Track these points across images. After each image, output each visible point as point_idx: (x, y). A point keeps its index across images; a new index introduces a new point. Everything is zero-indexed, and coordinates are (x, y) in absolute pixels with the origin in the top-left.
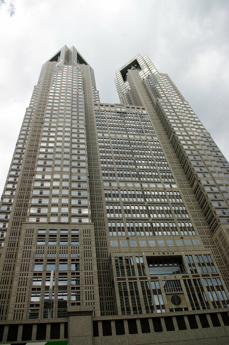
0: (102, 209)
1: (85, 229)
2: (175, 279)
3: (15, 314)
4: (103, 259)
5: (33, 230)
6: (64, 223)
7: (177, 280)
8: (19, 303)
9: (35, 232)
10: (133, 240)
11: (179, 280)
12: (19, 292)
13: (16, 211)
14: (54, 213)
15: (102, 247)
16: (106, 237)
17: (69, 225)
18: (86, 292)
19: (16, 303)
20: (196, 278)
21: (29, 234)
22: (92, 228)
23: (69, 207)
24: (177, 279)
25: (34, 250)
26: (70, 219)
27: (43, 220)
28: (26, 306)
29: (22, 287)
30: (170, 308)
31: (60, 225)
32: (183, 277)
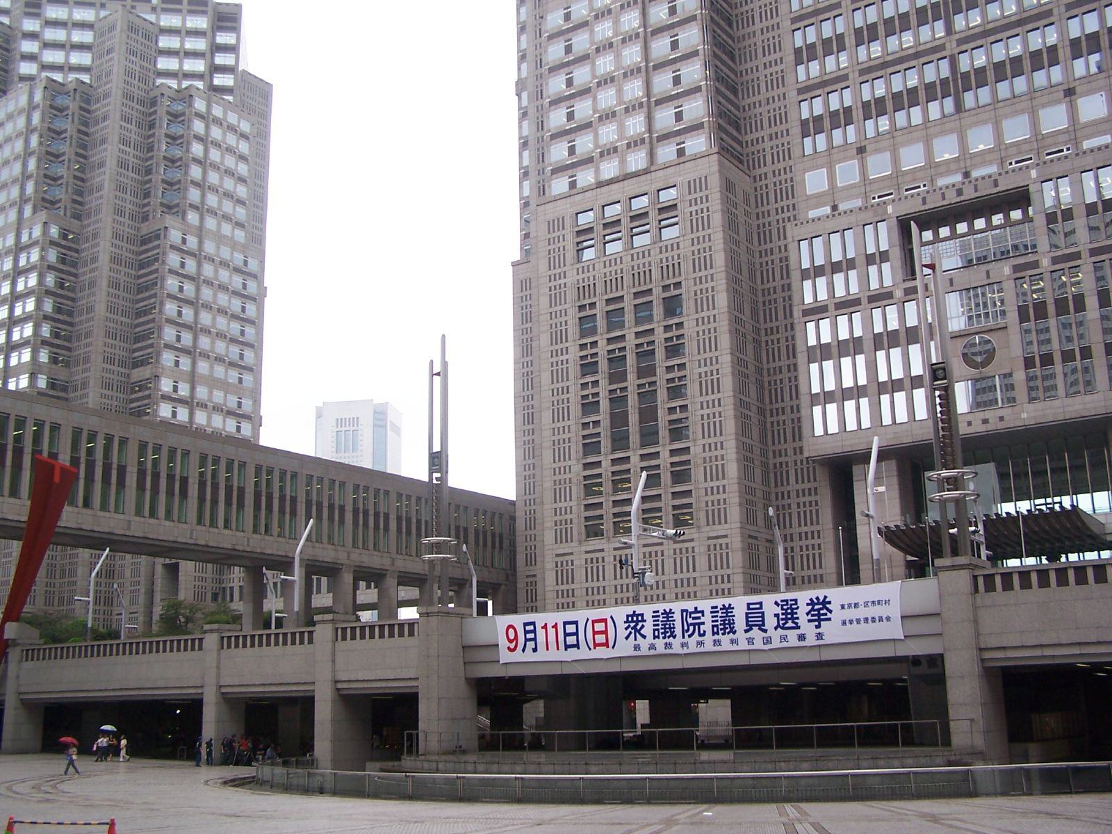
0: (778, 56)
1: (691, 177)
5: (563, 218)
6: (636, 175)
9: (568, 223)
10: (878, 151)
14: (608, 147)
16: (791, 163)
17: (648, 175)
18: (700, 374)
22: (711, 168)
23: (645, 109)
25: (572, 278)
26: (652, 155)
27: (586, 177)
28: (573, 429)
31: (626, 182)
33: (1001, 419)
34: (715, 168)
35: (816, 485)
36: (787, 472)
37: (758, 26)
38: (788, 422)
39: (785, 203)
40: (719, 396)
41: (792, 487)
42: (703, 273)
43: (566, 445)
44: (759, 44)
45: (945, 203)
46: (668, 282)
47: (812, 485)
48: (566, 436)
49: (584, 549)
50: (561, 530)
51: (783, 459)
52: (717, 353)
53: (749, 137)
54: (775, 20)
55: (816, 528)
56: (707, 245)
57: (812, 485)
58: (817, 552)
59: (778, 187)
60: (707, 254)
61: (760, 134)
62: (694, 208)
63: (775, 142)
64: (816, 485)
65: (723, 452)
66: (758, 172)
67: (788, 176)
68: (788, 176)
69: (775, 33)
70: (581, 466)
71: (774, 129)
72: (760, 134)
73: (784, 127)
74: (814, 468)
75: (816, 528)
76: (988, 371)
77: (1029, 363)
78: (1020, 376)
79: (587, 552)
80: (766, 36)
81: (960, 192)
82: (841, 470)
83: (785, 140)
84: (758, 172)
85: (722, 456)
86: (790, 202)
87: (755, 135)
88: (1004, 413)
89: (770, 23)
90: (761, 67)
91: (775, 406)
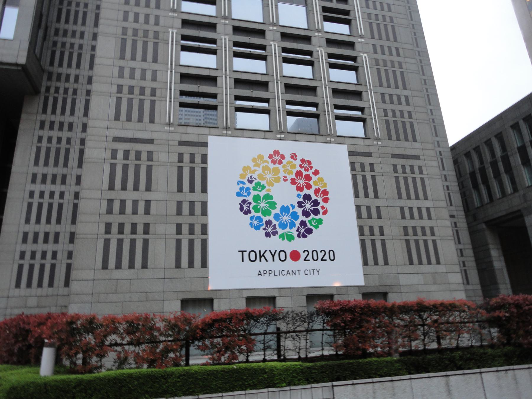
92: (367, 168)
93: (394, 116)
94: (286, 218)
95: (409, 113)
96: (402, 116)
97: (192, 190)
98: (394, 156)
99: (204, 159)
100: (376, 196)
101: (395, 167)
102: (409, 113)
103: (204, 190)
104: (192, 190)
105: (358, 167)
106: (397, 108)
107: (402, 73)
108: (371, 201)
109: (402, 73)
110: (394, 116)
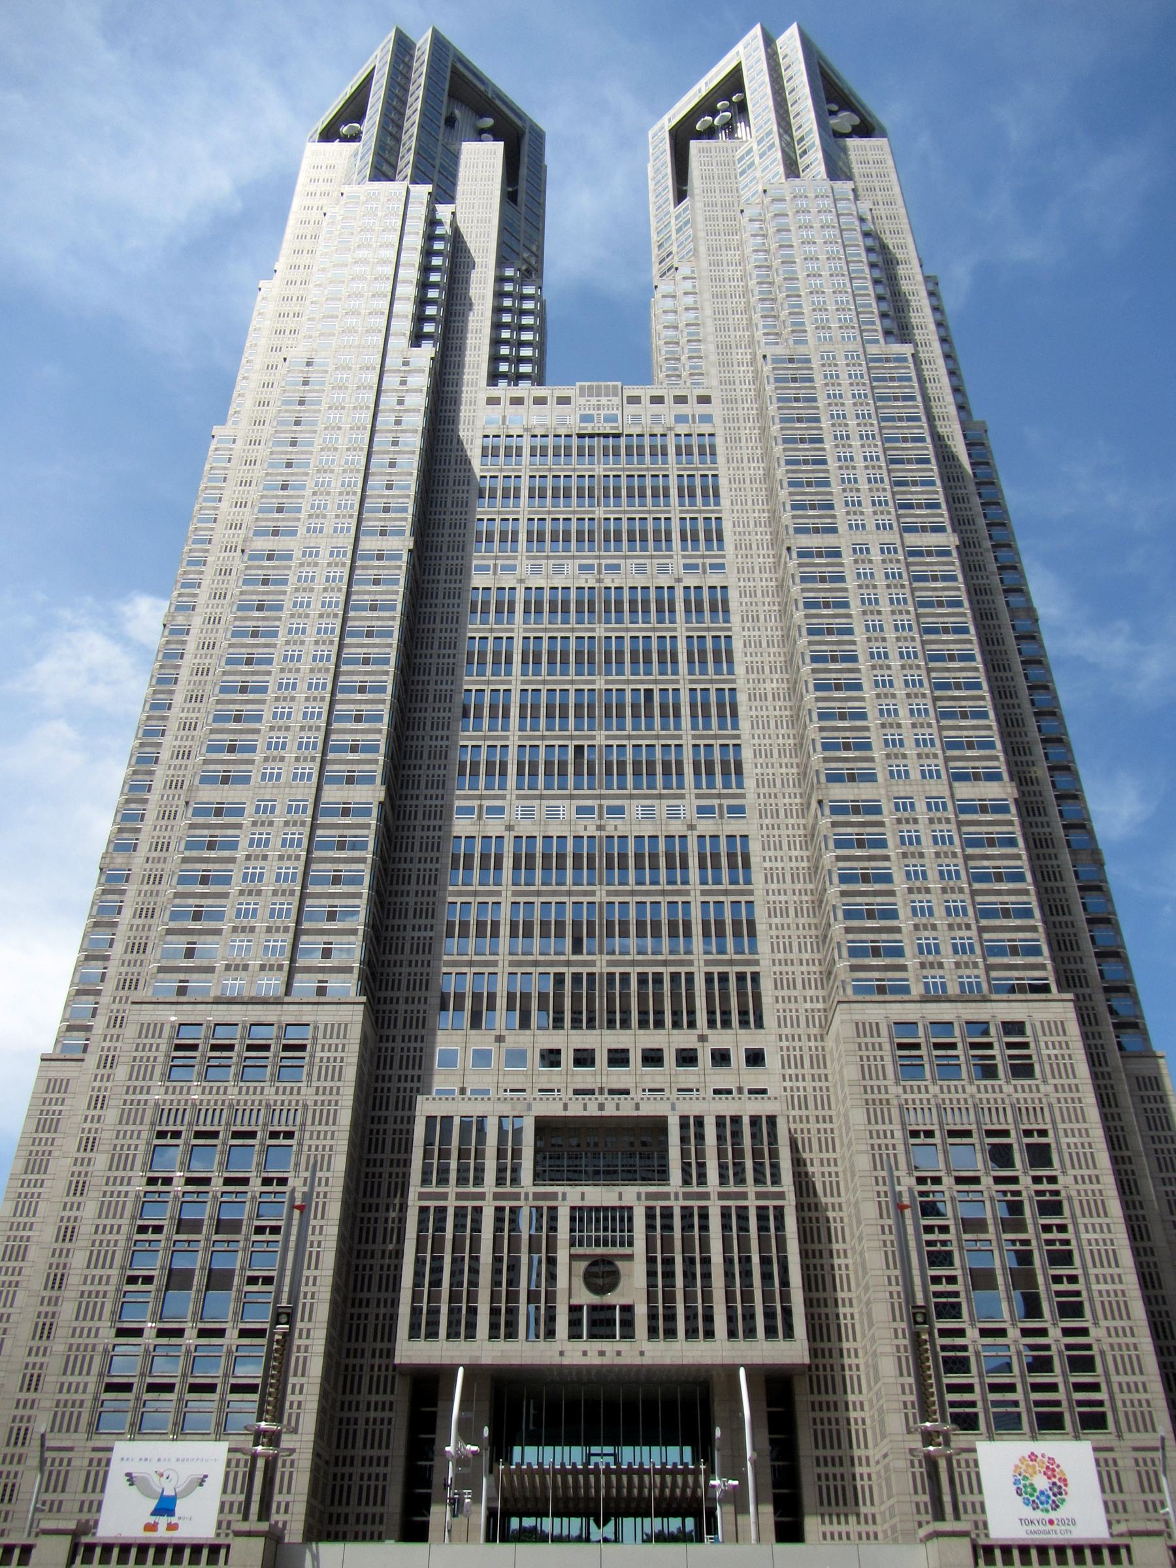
1: (329, 1020)
2: (617, 1204)
3: (80, 1304)
4: (399, 1113)
7: (622, 1208)
8: (95, 1272)
11: (630, 1208)
12: (99, 1237)
13: (132, 934)
15: (403, 1072)
19: (87, 1272)
20: (695, 1204)
21: (149, 1041)
24: (623, 1204)
29: (109, 1222)
30: (574, 1302)
32: (649, 1196)
33: (619, 1353)
34: (360, 1018)
35: (392, 1398)
36: (360, 1377)
37: (413, 887)
38: (372, 1318)
39: (410, 1072)
40: (316, 1273)
41: (364, 1397)
42: (323, 1128)
43: (99, 1300)
44: (412, 904)
45: (586, 1114)
46: (278, 1129)
47: (388, 1398)
48: (102, 1288)
49: (91, 1444)
50: (64, 1414)
51: (358, 1361)
52: (323, 1222)
53: (382, 994)
54: (432, 887)
55: (383, 1453)
56: (334, 1097)
57: (388, 1398)
58: (380, 1484)
59: (405, 1054)
60: (332, 1108)
61: (395, 994)
62: (326, 1054)
63: (410, 1007)
64: (392, 1398)
65: (308, 1342)
66: (386, 1032)
67: (418, 1045)
68: (418, 1045)
69: (431, 899)
70: (113, 1331)
71: (411, 994)
72: (395, 994)
73: (423, 994)
74: (393, 1378)
75: (383, 1453)
76: (611, 1298)
77: (651, 1297)
78: (641, 1311)
79: (95, 1449)
80: (420, 899)
81: (601, 1107)
82: (428, 1385)
83: (422, 1007)
84: (386, 1032)
85: (307, 1347)
86: (416, 1072)
87: (390, 994)
88: (624, 1346)
89: (426, 888)
90: (409, 928)
91: (359, 1295)
92: (1111, 1462)
93: (1133, 1405)
94: (1043, 1498)
95: (1148, 1401)
96: (1140, 1405)
97: (972, 1492)
98: (1136, 1449)
99: (976, 1462)
100: (1121, 1490)
101: (1136, 1460)
102: (1148, 1401)
103: (980, 1491)
104: (972, 1492)
105: (1102, 1463)
106: (1136, 1396)
107: (1138, 1357)
108: (1118, 1497)
109: (1138, 1357)
110: (1133, 1405)
